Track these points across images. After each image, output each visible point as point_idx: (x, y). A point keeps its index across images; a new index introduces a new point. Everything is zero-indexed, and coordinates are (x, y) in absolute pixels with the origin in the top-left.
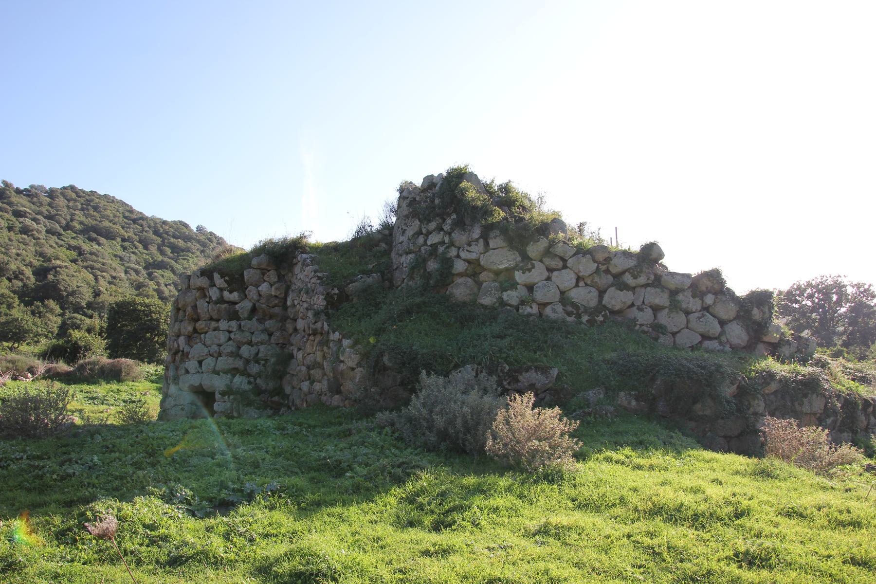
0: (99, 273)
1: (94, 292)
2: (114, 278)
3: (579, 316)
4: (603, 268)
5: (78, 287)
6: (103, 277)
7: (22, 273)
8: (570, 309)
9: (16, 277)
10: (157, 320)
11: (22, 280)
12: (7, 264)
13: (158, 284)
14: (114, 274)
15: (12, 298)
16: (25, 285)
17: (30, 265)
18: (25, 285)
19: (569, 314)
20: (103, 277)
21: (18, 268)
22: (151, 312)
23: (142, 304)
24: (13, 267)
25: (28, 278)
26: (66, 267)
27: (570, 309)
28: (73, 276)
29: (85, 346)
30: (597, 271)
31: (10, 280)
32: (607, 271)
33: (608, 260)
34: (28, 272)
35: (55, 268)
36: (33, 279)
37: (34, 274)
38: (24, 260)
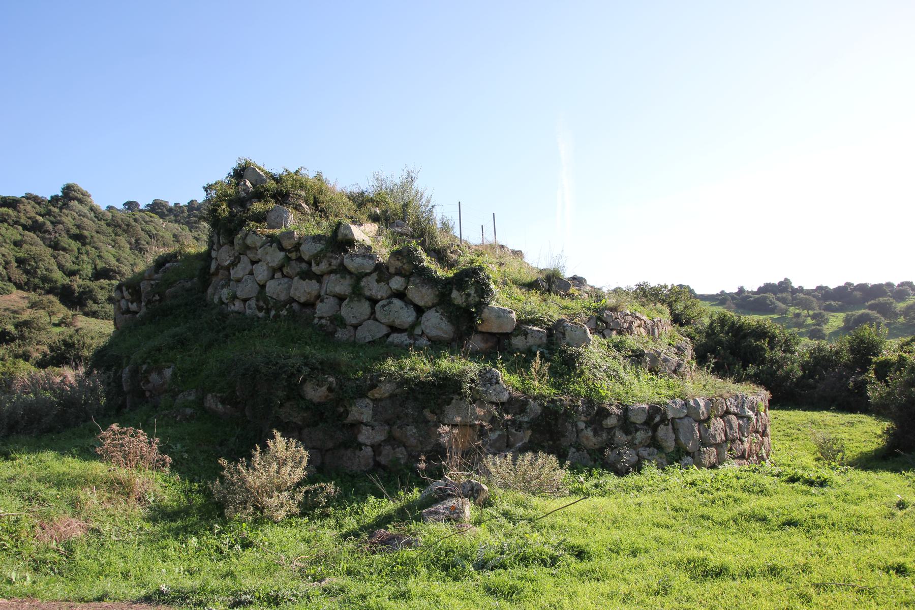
3: (268, 311)
4: (293, 255)
8: (261, 304)
19: (260, 309)
27: (261, 304)
30: (288, 259)
32: (300, 259)
33: (297, 247)
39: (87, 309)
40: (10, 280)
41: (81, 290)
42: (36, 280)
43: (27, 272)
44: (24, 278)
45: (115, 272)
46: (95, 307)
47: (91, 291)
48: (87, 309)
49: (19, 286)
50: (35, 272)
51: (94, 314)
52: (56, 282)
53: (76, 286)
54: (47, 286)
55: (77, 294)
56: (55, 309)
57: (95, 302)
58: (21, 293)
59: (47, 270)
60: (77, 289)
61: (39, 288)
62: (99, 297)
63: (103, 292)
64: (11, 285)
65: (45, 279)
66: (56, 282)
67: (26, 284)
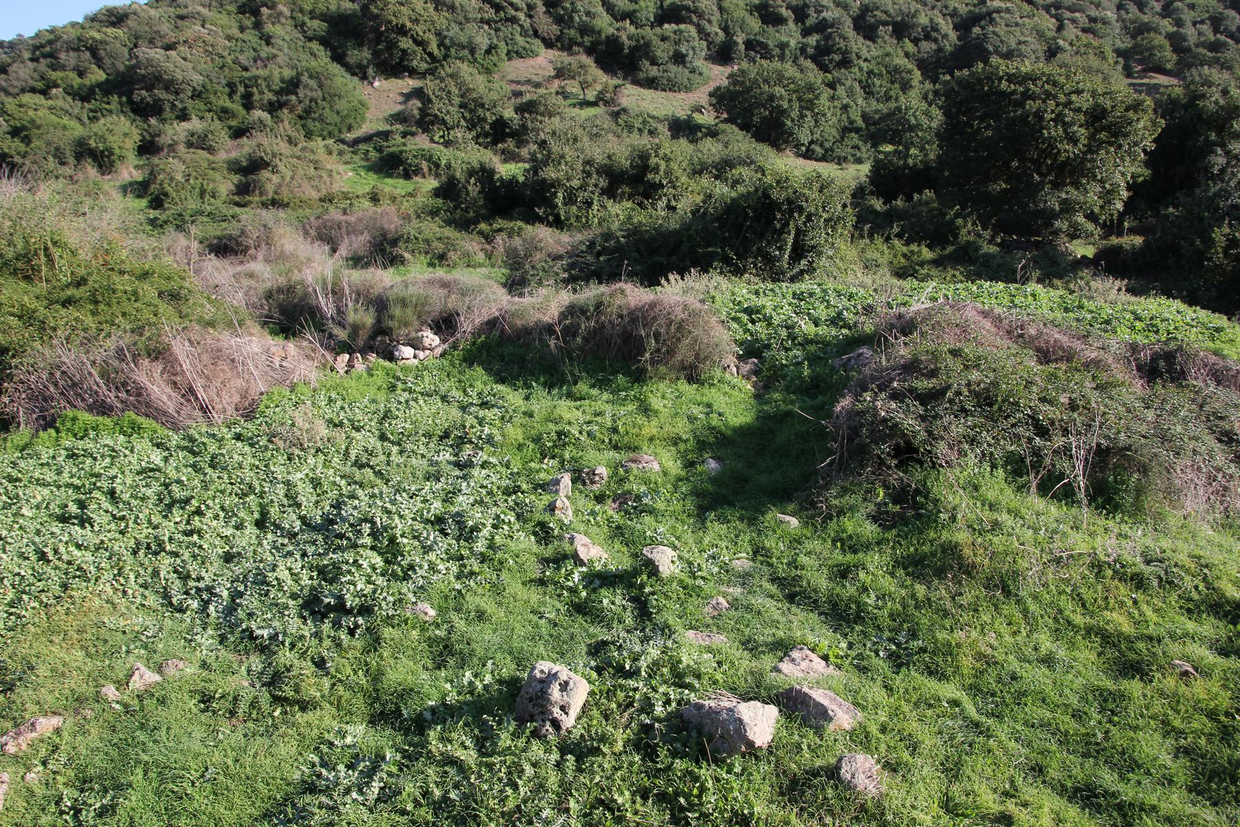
0: (1067, 14)
1: (1049, 49)
2: (1093, 20)
5: (1020, 43)
6: (1073, 21)
7: (935, 28)
9: (927, 37)
10: (1039, 116)
11: (936, 41)
12: (914, 16)
13: (1179, 23)
14: (1093, 13)
15: (909, 72)
16: (940, 50)
17: (954, 14)
18: (940, 50)
20: (1073, 21)
21: (931, 20)
22: (1027, 95)
23: (1011, 79)
24: (923, 20)
25: (945, 36)
26: (1008, 10)
28: (1017, 24)
29: (789, 201)
31: (915, 41)
34: (946, 26)
35: (989, 14)
36: (953, 35)
37: (956, 28)
38: (946, 7)
39: (642, 75)
40: (536, 34)
41: (634, 43)
42: (572, 32)
43: (559, 20)
44: (555, 29)
45: (688, 9)
46: (654, 71)
47: (648, 45)
48: (642, 75)
49: (549, 44)
50: (571, 18)
51: (651, 83)
52: (599, 32)
53: (624, 38)
54: (587, 40)
55: (626, 51)
56: (590, 79)
57: (654, 62)
58: (553, 54)
59: (588, 13)
60: (627, 42)
61: (576, 44)
62: (659, 53)
63: (666, 45)
64: (538, 42)
65: (585, 30)
66: (599, 32)
67: (559, 39)
